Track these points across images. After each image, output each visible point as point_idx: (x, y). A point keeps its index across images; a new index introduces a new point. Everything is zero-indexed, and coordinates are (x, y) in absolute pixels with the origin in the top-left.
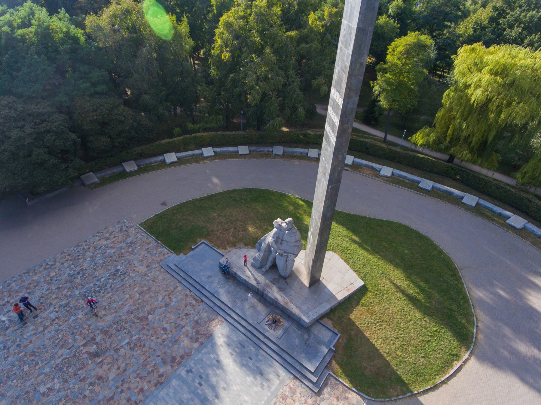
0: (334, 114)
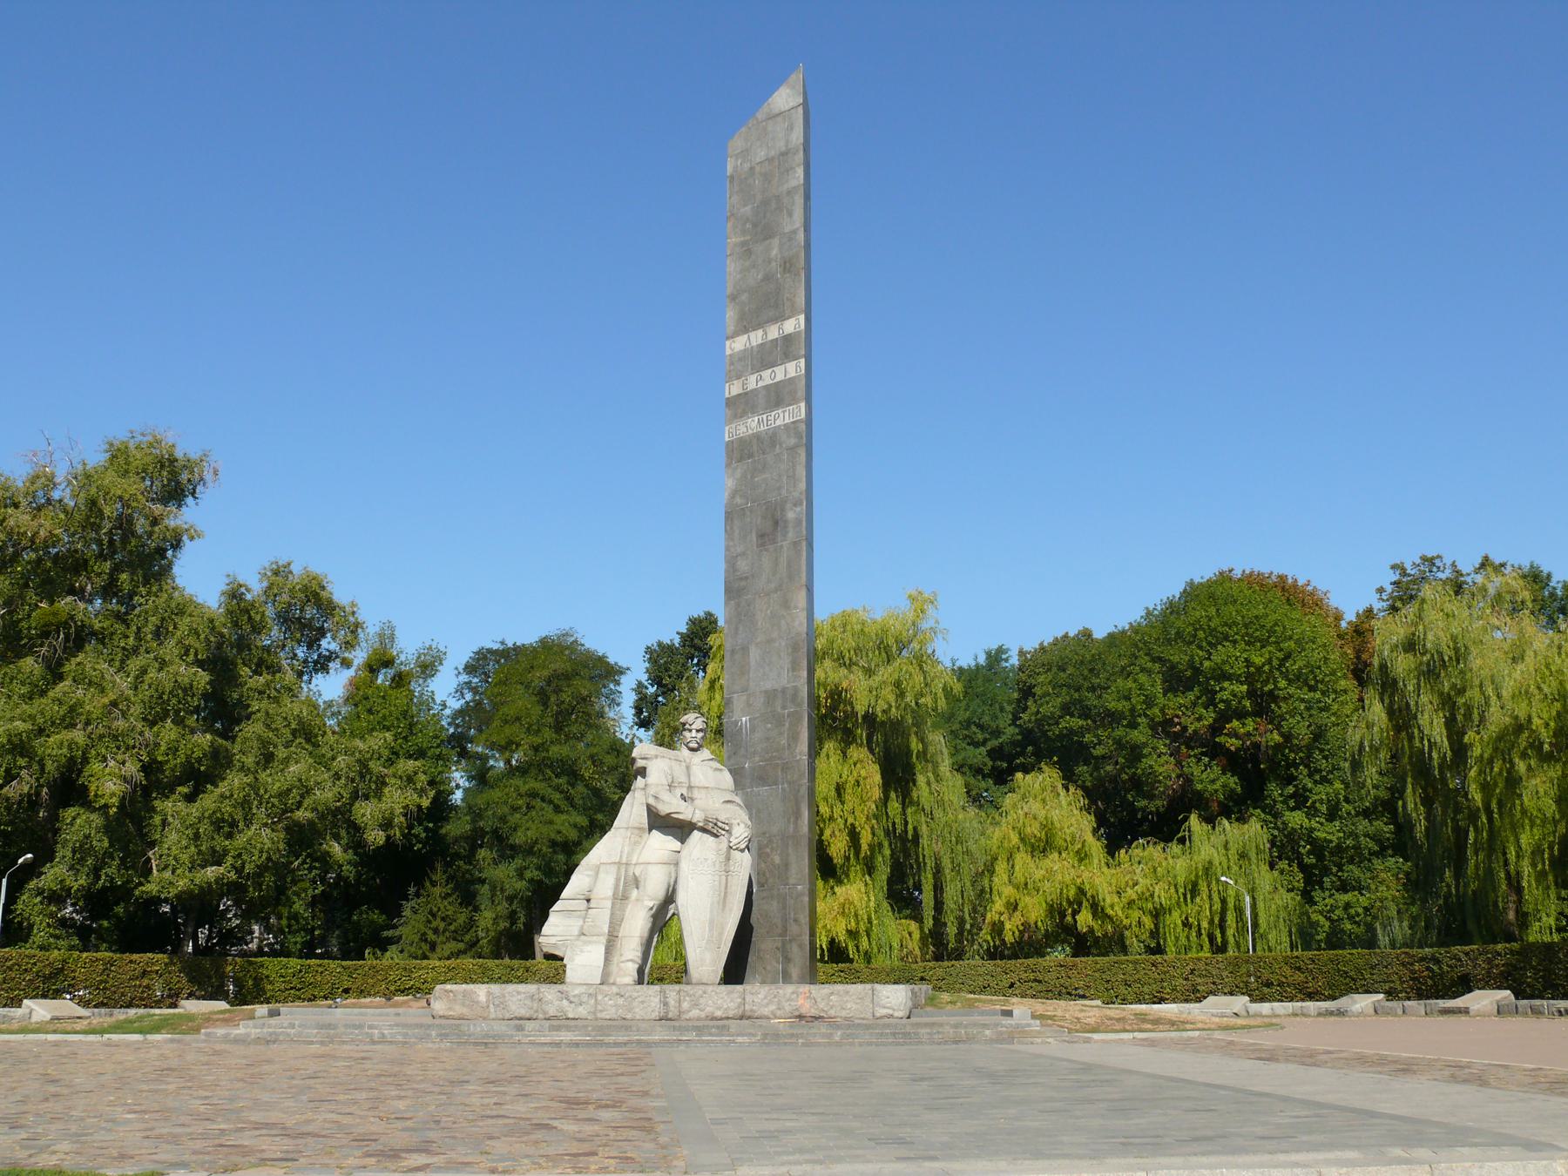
0: (766, 374)
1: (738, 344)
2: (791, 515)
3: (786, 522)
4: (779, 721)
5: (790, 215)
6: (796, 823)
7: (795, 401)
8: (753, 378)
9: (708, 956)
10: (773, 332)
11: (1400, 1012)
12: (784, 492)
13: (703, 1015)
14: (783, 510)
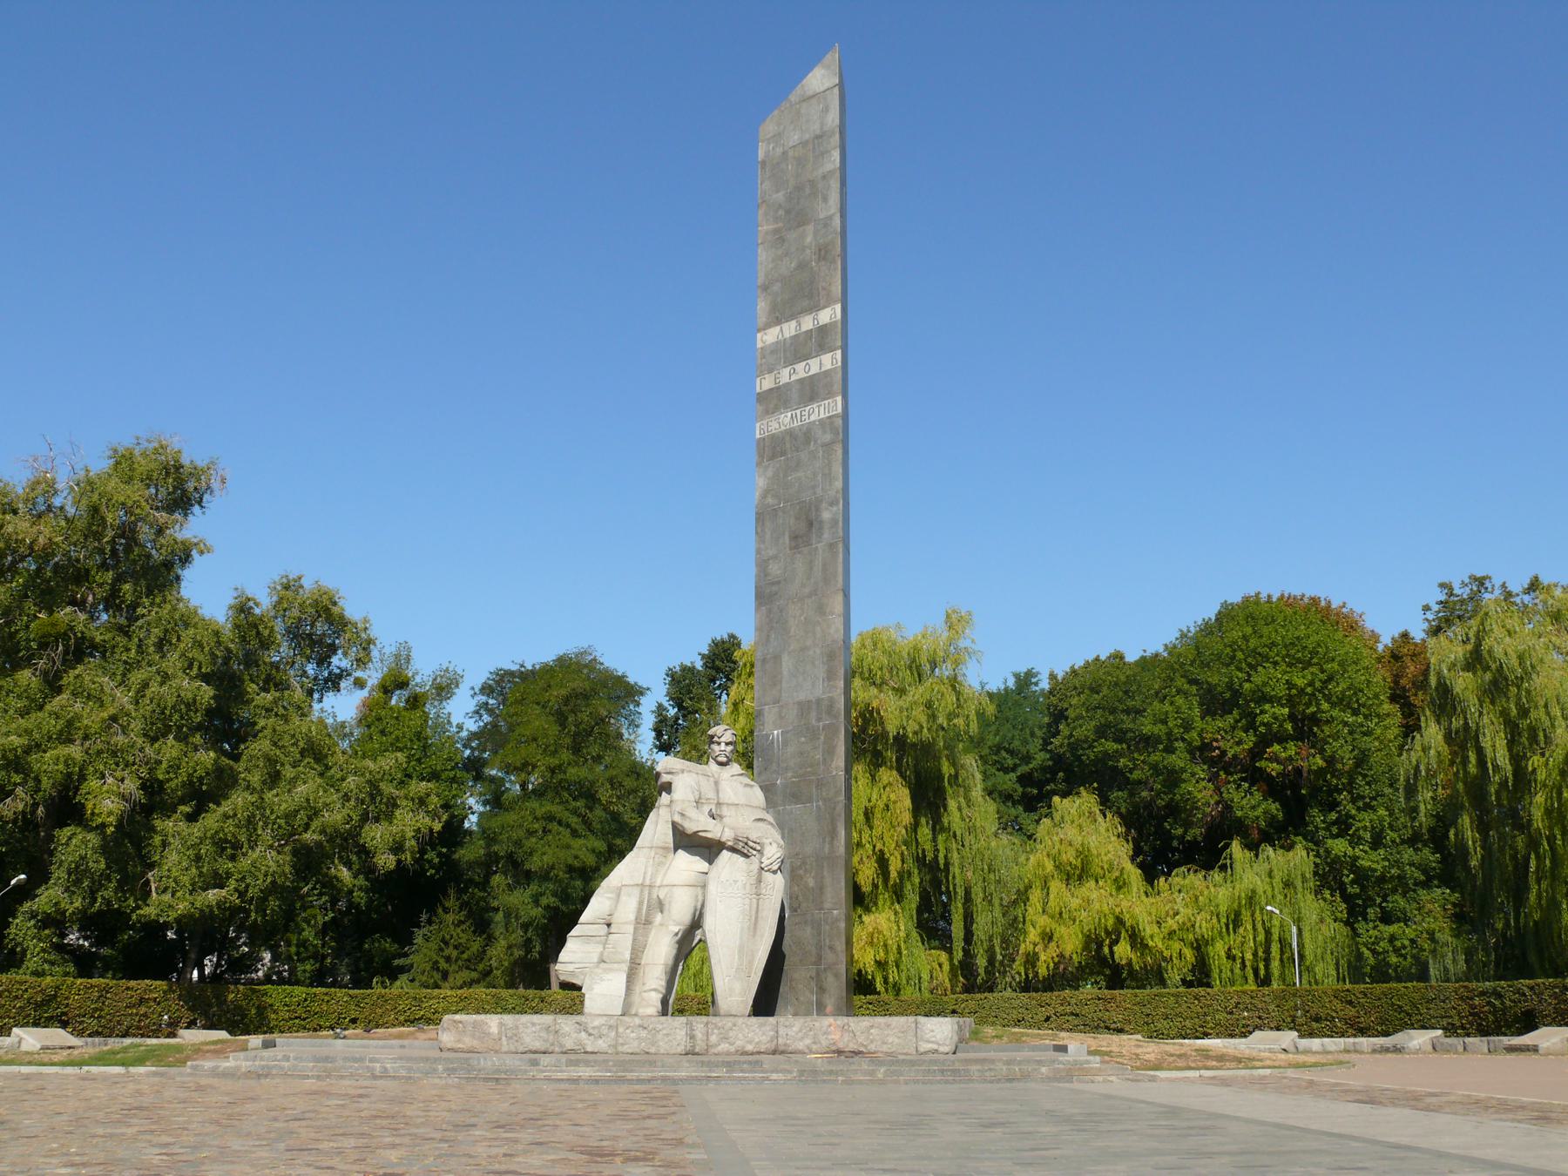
0: (800, 367)
1: (770, 336)
2: (826, 516)
3: (821, 522)
5: (825, 199)
6: (831, 843)
7: (830, 395)
8: (786, 371)
9: (737, 986)
10: (808, 323)
11: (1461, 1049)
12: (819, 491)
13: (732, 1049)
14: (818, 510)
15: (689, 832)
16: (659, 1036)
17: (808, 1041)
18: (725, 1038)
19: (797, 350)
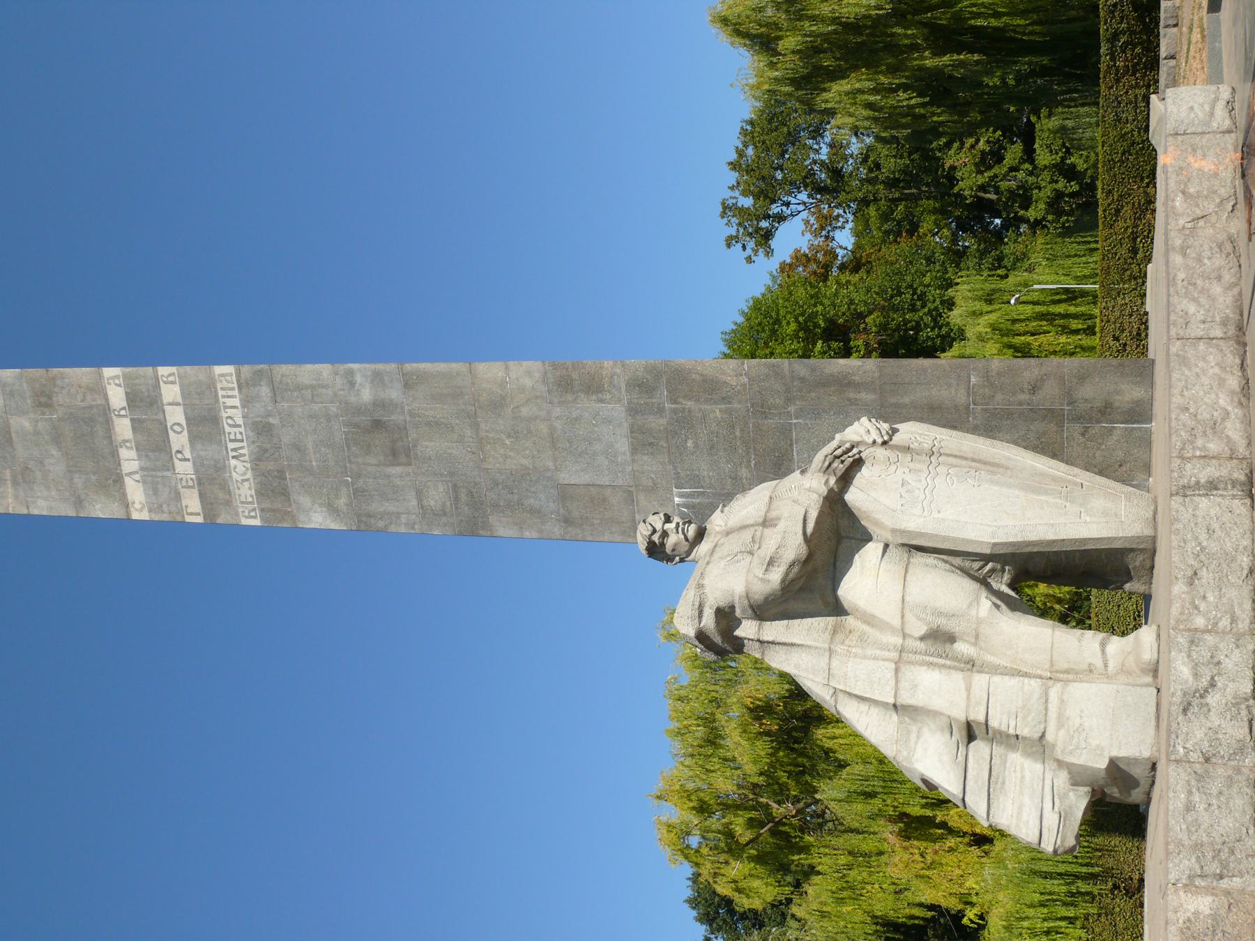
1: (135, 492)
2: (366, 395)
4: (683, 422)
6: (857, 386)
7: (211, 386)
9: (1099, 503)
10: (123, 428)
11: (1172, 63)
12: (333, 409)
13: (1235, 412)
14: (359, 410)
15: (804, 550)
16: (1213, 547)
17: (1217, 289)
18: (1214, 427)
19: (155, 444)
